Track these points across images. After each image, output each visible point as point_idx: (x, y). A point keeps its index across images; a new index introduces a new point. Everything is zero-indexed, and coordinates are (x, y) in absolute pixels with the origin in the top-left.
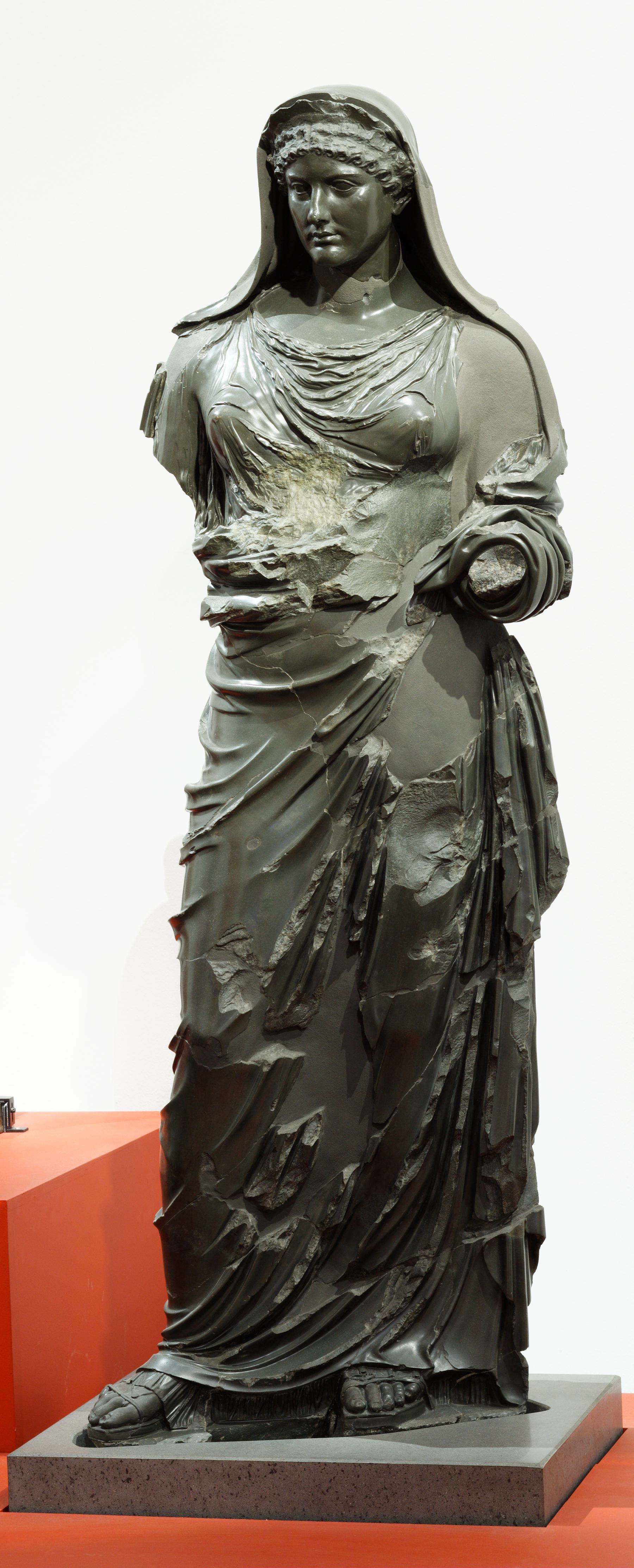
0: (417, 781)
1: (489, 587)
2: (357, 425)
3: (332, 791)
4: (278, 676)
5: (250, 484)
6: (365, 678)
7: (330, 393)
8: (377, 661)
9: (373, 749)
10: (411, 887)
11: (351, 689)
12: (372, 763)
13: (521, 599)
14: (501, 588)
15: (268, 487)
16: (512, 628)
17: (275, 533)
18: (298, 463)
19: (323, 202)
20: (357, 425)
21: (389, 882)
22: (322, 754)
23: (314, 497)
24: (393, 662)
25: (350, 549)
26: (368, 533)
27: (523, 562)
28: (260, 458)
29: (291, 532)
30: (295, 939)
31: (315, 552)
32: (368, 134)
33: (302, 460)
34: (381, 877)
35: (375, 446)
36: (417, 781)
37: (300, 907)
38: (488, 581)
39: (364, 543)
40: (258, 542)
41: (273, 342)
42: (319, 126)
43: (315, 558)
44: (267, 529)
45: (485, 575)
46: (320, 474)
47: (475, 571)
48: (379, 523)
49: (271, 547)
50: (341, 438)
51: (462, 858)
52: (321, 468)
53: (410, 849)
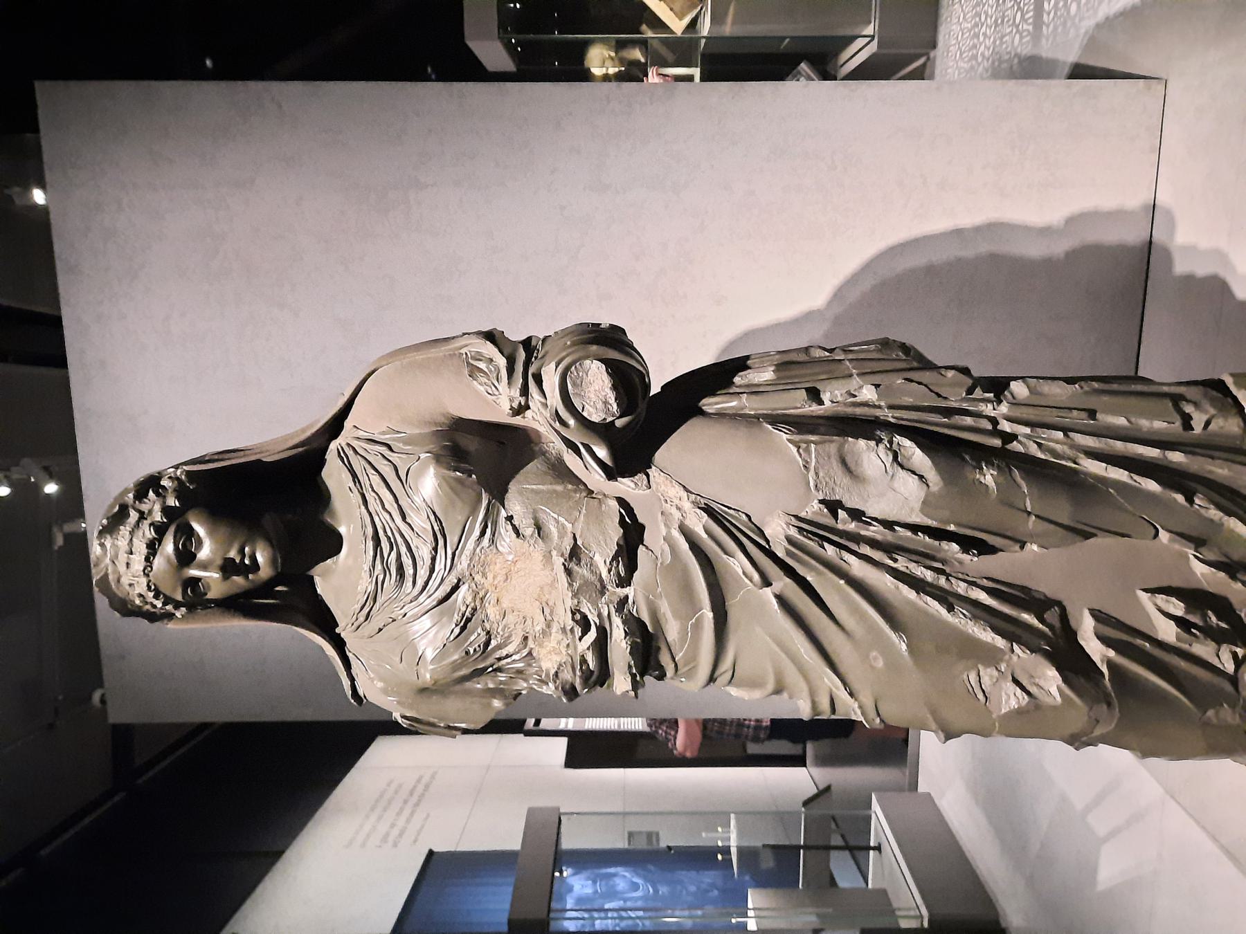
0: (812, 484)
1: (612, 400)
2: (439, 536)
3: (819, 573)
4: (698, 626)
5: (499, 647)
6: (705, 536)
7: (407, 561)
8: (687, 522)
9: (777, 531)
10: (923, 495)
11: (1159, 687)
12: (793, 532)
13: (628, 378)
14: (615, 387)
15: (503, 630)
16: (655, 389)
17: (549, 626)
18: (480, 597)
19: (204, 566)
20: (439, 536)
21: (917, 518)
22: (781, 583)
23: (514, 582)
24: (687, 505)
25: (569, 548)
26: (553, 529)
27: (587, 362)
28: (472, 638)
29: (546, 609)
30: (975, 618)
31: (570, 585)
32: (134, 516)
33: (476, 594)
34: (915, 528)
35: (461, 518)
36: (812, 484)
37: (943, 611)
38: (606, 403)
39: (562, 531)
40: (559, 643)
41: (362, 619)
42: (122, 568)
43: (576, 585)
44: (546, 633)
45: (600, 405)
46: (490, 576)
47: (596, 418)
48: (542, 516)
49: (564, 630)
50: (454, 555)
51: (891, 442)
52: (484, 575)
53: (882, 495)
